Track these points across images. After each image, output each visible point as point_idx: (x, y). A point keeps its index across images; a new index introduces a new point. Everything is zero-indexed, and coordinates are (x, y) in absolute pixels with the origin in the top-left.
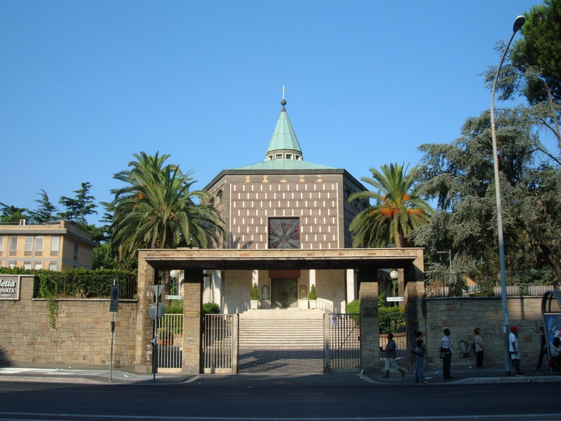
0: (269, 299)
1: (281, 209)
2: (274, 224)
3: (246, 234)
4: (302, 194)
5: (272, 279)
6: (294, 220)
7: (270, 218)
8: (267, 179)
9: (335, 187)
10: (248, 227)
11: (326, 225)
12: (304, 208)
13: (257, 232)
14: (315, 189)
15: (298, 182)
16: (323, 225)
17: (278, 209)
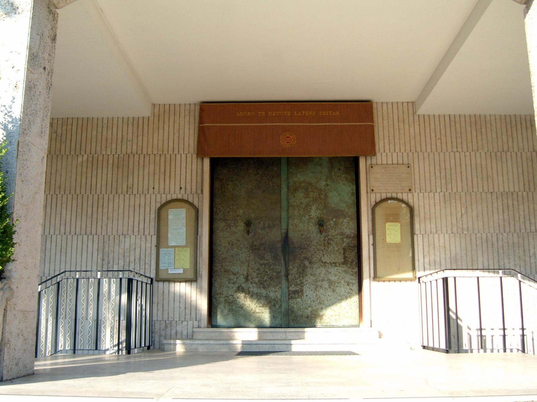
0: (193, 280)
5: (215, 163)
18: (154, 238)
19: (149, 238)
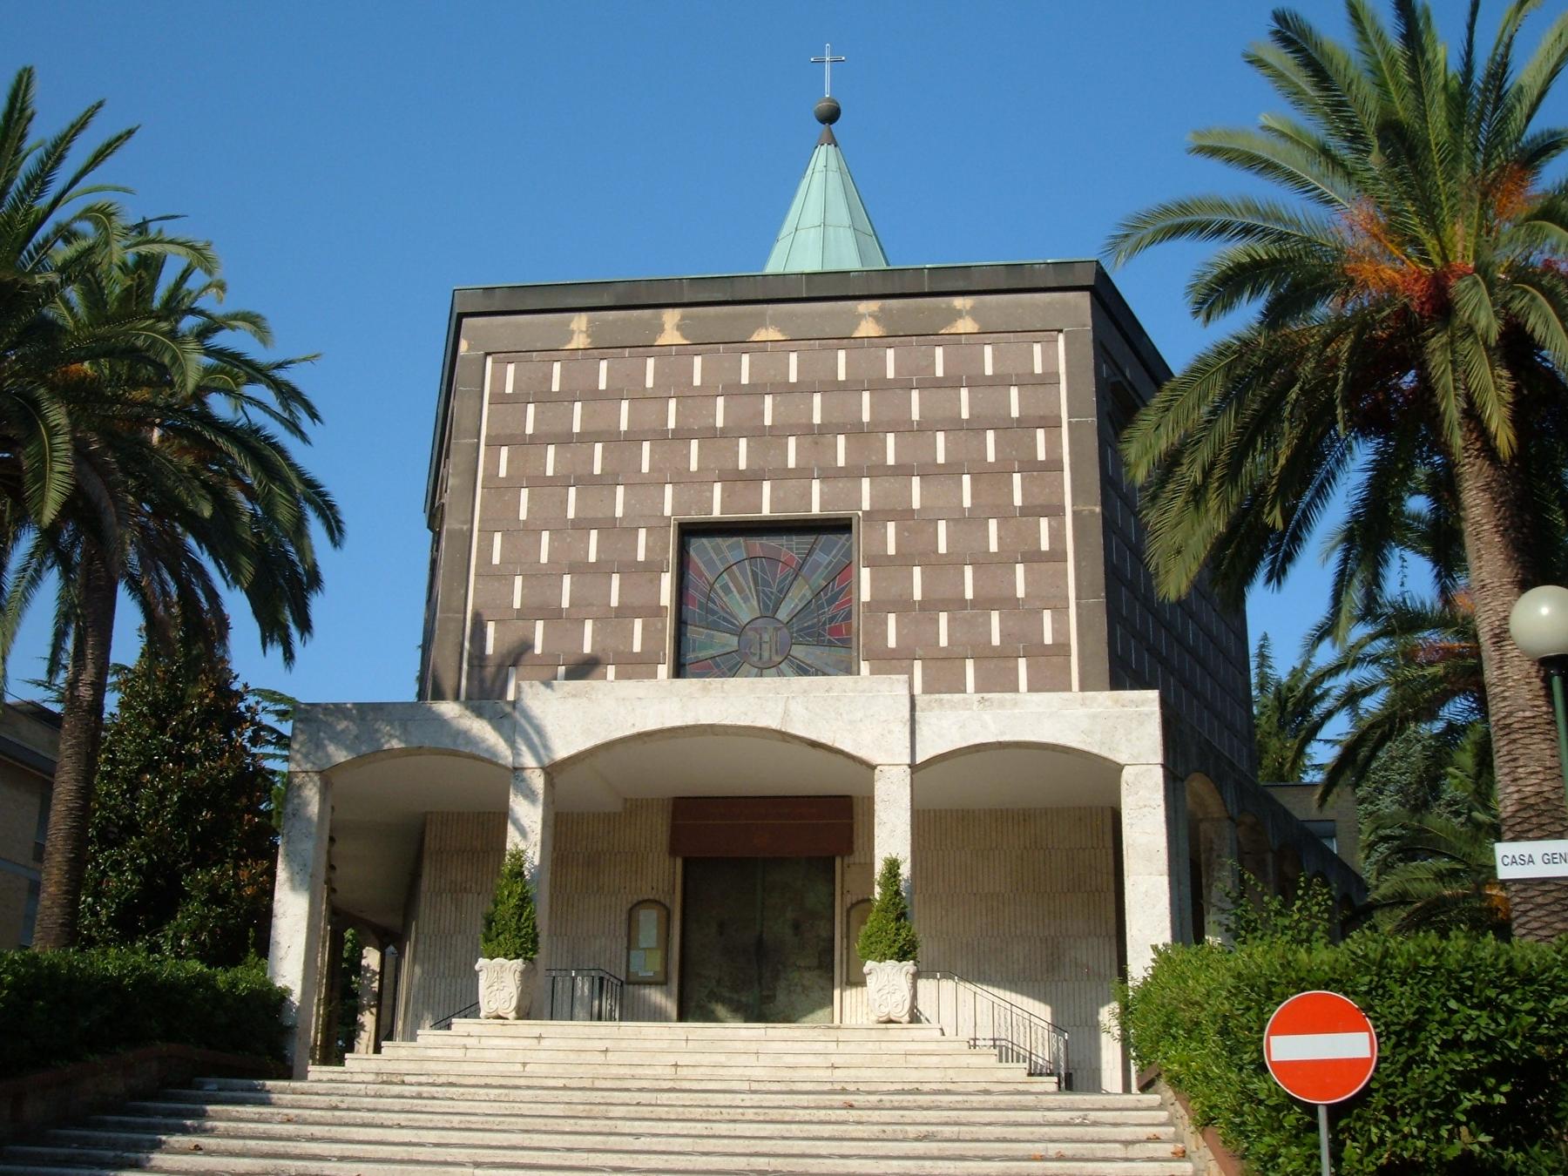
0: (661, 982)
1: (753, 478)
2: (710, 564)
3: (552, 614)
4: (866, 396)
5: (687, 863)
6: (823, 538)
7: (688, 531)
8: (679, 328)
9: (1050, 358)
10: (567, 579)
11: (1005, 561)
12: (878, 471)
13: (614, 602)
14: (939, 372)
15: (845, 339)
16: (982, 562)
17: (732, 478)
18: (625, 939)
19: (619, 940)
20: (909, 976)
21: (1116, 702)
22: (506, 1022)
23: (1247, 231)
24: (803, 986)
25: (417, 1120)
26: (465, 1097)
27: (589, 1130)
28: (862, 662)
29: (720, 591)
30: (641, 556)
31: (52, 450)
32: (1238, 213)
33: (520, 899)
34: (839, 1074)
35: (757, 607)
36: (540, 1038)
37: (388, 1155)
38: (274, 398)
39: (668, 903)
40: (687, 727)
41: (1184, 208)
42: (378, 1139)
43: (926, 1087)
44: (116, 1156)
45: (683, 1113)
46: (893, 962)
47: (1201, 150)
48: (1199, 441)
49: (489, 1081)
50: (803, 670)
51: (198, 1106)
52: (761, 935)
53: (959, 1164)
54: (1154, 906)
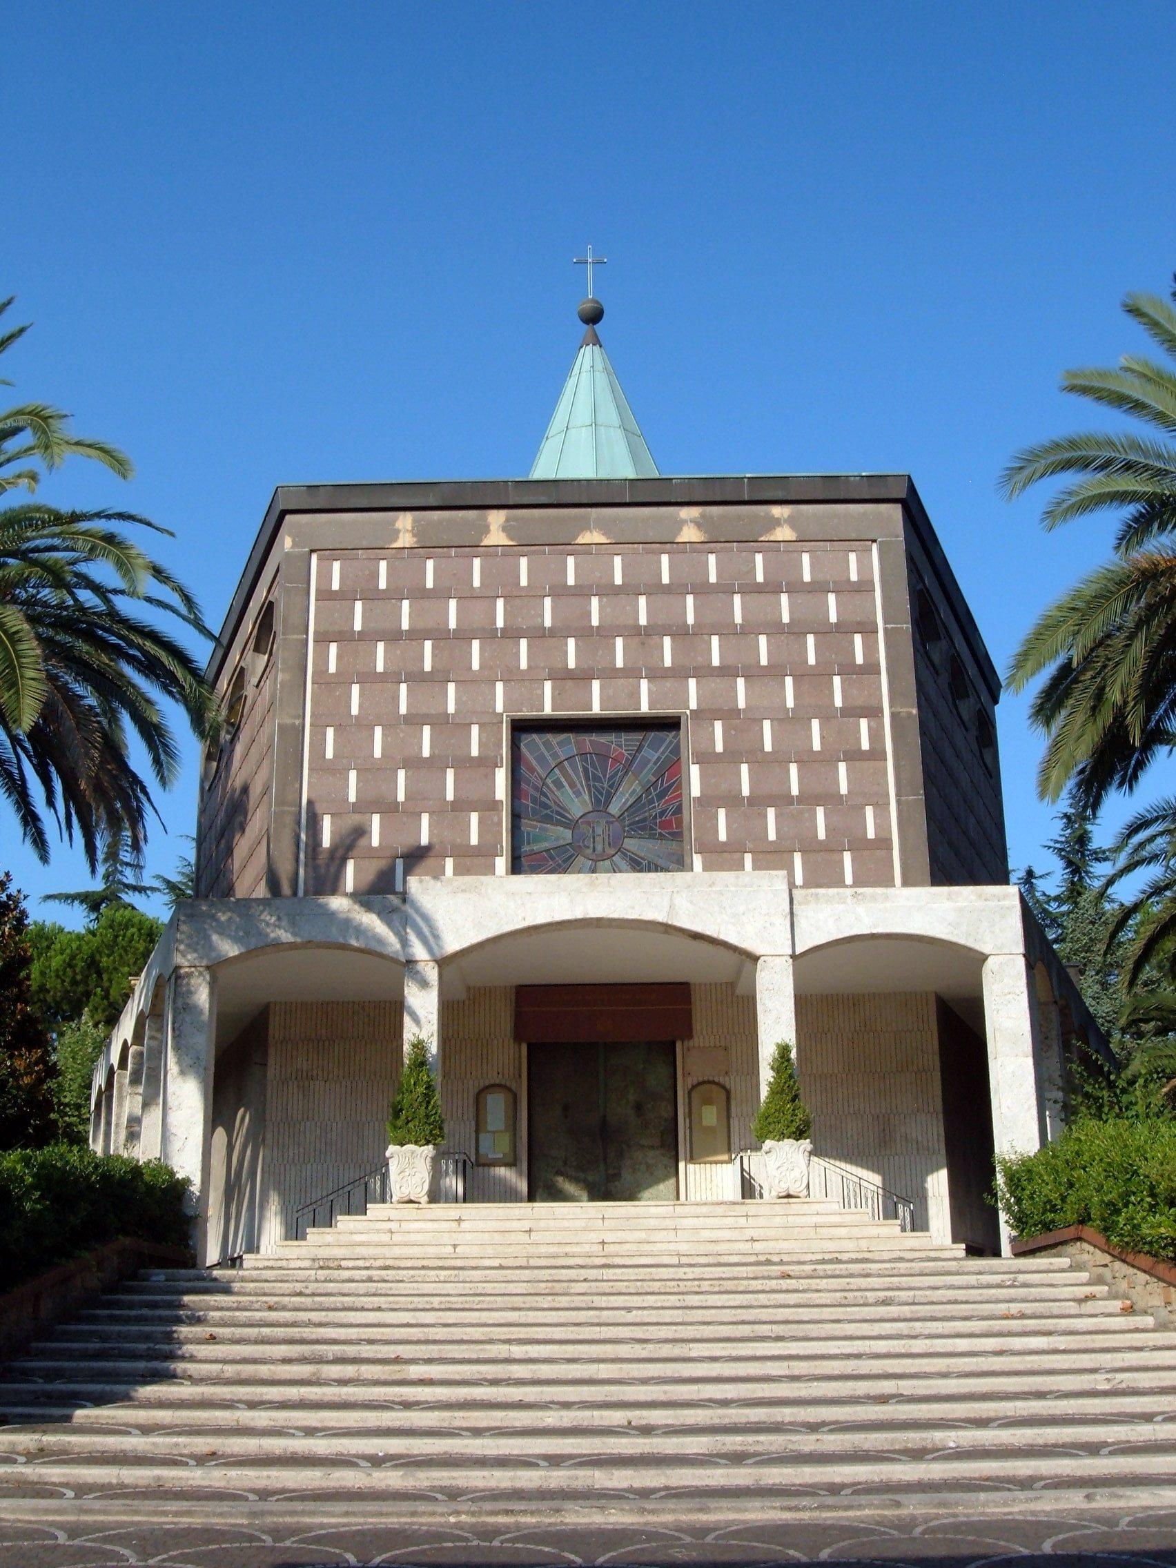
0: (512, 1163)
1: (583, 677)
2: (541, 759)
3: (389, 808)
4: (690, 599)
6: (652, 735)
7: (520, 727)
8: (504, 529)
9: (864, 566)
10: (401, 774)
11: (828, 759)
12: (704, 672)
13: (450, 796)
14: (760, 578)
15: (668, 544)
16: (807, 760)
17: (562, 676)
18: (473, 1123)
19: (467, 1123)
20: (807, 1154)
21: (980, 896)
22: (421, 1206)
23: (1129, 466)
24: (646, 1163)
25: (397, 1303)
26: (416, 1279)
27: (567, 1305)
28: (694, 855)
29: (552, 786)
30: (475, 752)
31: (18, 657)
32: (1121, 449)
33: (426, 1088)
34: (758, 1247)
35: (588, 801)
36: (459, 1220)
37: (405, 1337)
38: (180, 600)
39: (514, 1087)
40: (576, 920)
41: (1073, 444)
42: (376, 1321)
43: (844, 1257)
44: (149, 1348)
45: (642, 1287)
46: (791, 1141)
47: (1072, 389)
48: (1117, 664)
49: (425, 1263)
50: (638, 865)
51: (174, 1298)
52: (605, 1116)
53: (945, 1324)
54: (1021, 1085)
